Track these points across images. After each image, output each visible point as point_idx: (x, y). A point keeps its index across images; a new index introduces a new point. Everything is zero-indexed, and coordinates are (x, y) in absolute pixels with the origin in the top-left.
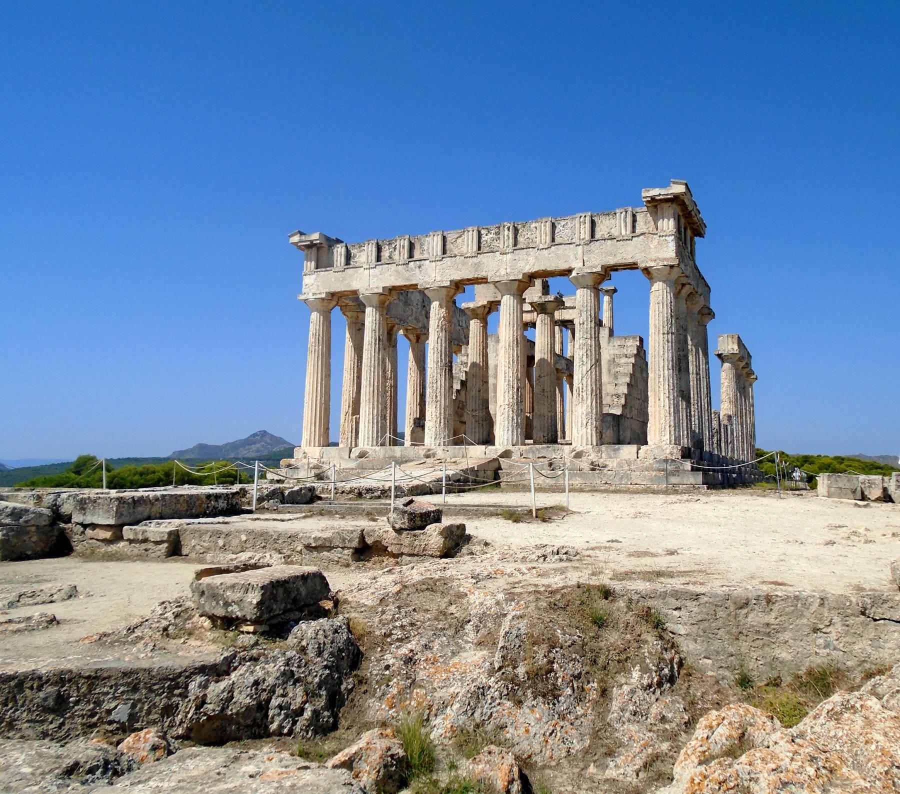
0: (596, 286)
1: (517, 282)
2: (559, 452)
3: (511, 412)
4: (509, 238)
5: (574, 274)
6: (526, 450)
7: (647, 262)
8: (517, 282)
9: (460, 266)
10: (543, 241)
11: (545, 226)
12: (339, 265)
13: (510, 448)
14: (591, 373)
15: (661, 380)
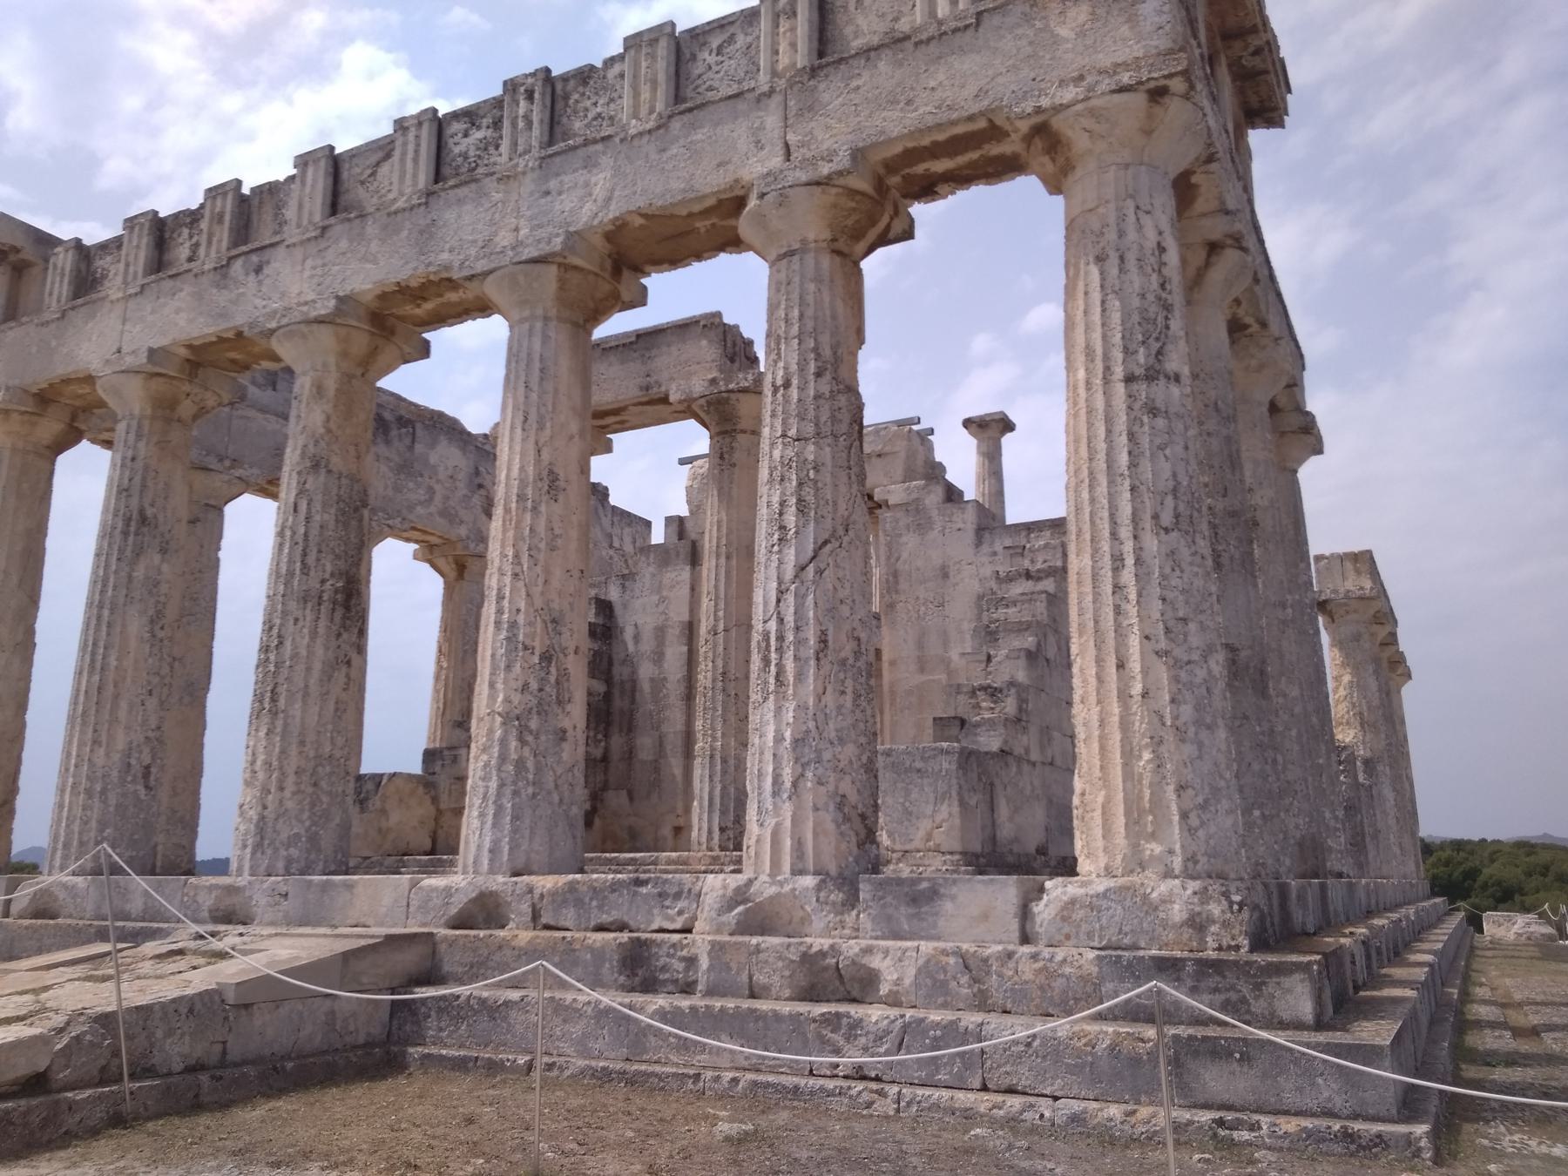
0: (841, 245)
1: (552, 271)
2: (680, 905)
3: (513, 744)
4: (529, 124)
5: (753, 203)
6: (554, 893)
7: (1042, 93)
8: (553, 269)
9: (374, 247)
10: (644, 112)
11: (652, 56)
12: (54, 304)
13: (500, 882)
14: (819, 572)
15: (1128, 576)
